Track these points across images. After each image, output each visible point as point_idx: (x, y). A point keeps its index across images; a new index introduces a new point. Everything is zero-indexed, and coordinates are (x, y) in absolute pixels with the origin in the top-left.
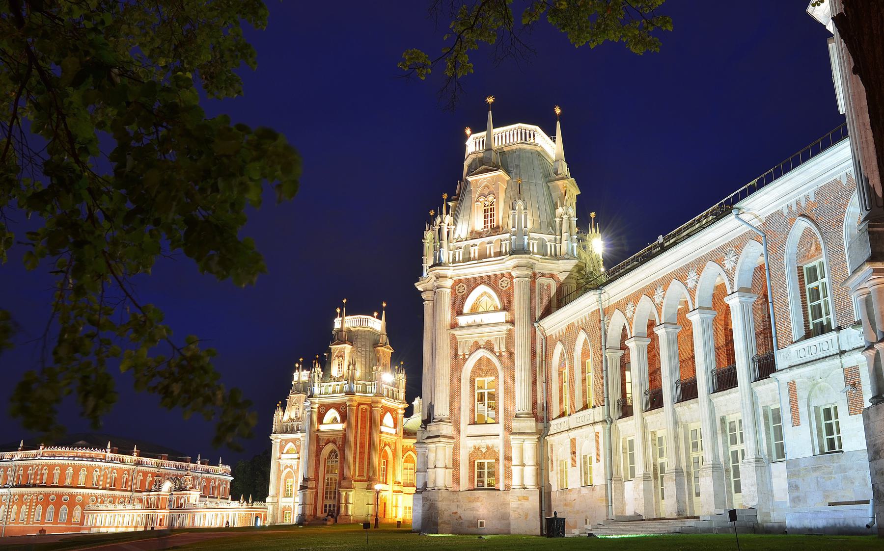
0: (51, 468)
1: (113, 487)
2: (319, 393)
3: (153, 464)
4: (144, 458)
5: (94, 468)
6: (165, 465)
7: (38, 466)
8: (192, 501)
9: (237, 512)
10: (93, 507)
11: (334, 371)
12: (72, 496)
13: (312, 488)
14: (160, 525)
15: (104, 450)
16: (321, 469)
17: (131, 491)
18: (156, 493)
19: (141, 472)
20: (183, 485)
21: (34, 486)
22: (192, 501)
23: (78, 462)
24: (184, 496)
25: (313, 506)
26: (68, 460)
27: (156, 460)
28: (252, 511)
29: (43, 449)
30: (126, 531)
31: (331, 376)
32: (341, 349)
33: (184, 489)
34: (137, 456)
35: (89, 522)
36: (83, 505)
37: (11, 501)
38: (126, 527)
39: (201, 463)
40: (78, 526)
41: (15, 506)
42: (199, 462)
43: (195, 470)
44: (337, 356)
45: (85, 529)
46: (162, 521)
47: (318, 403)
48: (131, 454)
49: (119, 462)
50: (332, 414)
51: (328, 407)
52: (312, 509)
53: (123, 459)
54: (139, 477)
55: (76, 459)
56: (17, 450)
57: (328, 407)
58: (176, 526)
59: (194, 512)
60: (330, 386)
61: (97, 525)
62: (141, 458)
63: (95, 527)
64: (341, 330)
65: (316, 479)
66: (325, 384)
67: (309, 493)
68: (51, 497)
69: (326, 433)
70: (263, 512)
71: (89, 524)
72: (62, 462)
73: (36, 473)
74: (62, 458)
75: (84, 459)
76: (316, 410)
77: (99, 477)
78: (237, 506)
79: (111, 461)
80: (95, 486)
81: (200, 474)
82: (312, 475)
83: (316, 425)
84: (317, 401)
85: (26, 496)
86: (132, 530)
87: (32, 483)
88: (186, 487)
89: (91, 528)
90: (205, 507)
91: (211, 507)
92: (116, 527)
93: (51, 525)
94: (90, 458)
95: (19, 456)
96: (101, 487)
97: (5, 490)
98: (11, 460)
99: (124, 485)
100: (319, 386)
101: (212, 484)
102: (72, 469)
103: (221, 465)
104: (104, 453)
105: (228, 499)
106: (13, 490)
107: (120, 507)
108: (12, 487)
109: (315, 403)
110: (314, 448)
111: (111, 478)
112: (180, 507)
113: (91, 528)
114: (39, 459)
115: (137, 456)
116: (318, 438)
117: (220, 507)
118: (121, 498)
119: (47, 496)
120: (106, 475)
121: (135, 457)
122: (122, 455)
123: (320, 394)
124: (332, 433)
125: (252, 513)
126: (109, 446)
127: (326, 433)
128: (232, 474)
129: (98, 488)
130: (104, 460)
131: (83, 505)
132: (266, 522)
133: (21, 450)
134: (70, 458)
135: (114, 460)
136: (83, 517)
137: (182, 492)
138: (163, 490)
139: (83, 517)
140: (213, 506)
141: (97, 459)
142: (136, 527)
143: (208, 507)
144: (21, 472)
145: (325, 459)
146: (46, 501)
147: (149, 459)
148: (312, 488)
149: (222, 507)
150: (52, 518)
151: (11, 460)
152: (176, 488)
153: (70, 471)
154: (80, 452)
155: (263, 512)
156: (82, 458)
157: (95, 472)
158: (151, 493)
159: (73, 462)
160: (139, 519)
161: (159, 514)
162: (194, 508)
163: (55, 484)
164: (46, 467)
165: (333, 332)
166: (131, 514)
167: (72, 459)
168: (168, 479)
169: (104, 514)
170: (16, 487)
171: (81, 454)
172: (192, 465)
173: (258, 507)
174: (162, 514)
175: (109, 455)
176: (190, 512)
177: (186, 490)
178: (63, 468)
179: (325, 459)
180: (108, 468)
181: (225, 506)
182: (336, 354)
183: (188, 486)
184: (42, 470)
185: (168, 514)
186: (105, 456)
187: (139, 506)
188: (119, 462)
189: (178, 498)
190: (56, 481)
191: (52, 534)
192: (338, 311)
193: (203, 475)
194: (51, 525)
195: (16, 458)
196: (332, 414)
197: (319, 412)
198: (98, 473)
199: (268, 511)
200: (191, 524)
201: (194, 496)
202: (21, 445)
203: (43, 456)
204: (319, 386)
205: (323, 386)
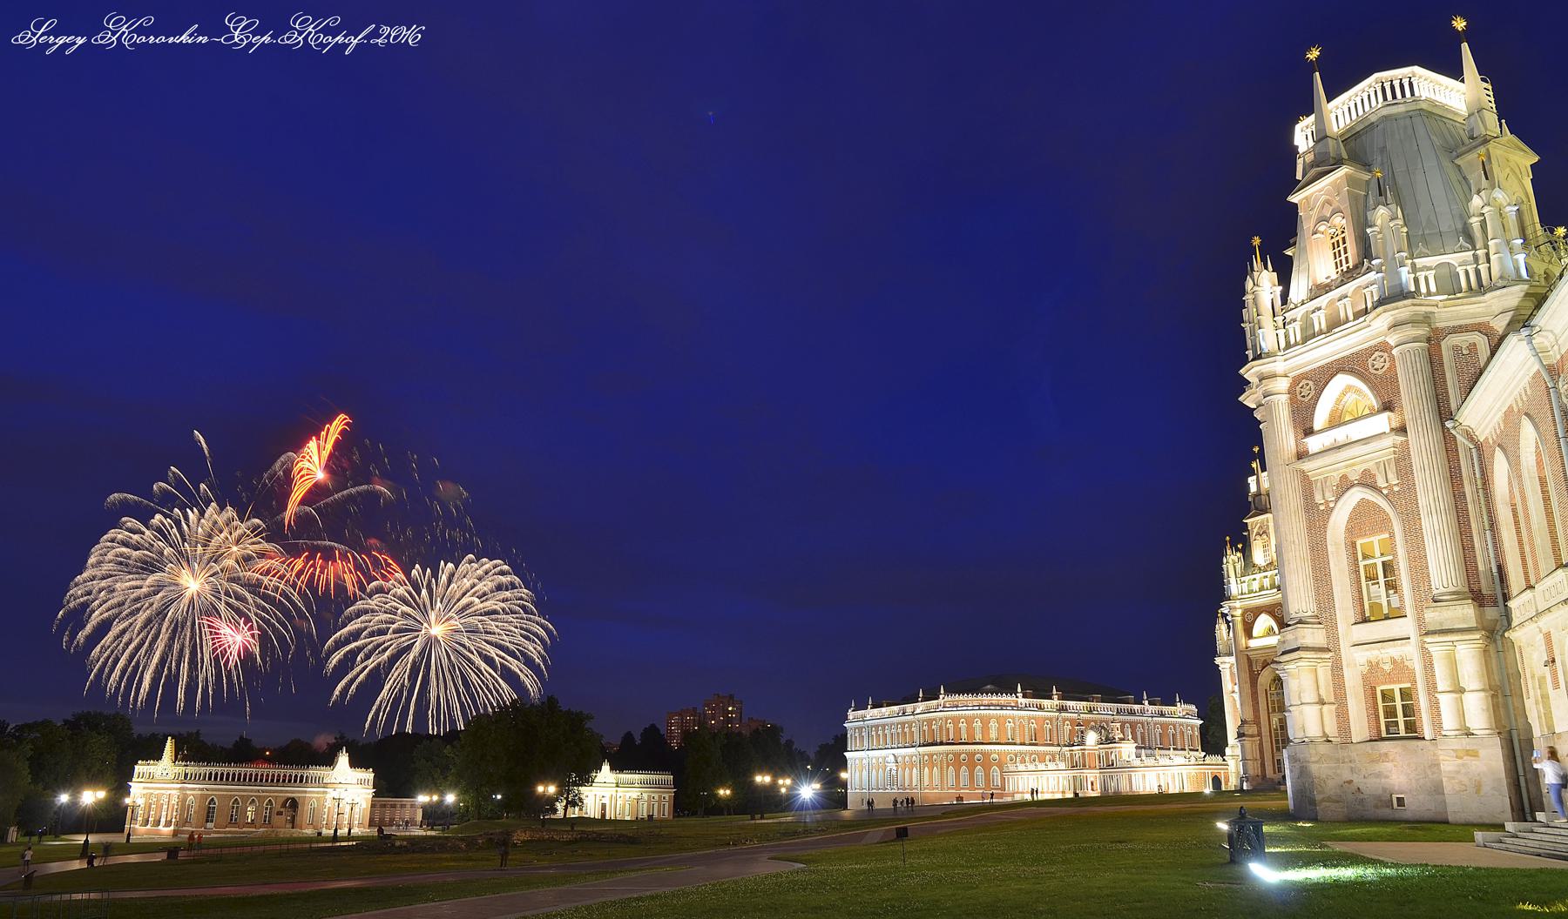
0: (956, 720)
2: (1240, 592)
5: (1005, 718)
7: (941, 719)
8: (1125, 757)
9: (1185, 771)
10: (1012, 768)
11: (1259, 557)
12: (986, 754)
13: (1252, 736)
14: (1093, 790)
17: (1059, 745)
18: (1079, 747)
19: (1067, 720)
20: (1110, 736)
21: (942, 744)
22: (1125, 757)
23: (985, 712)
25: (1259, 762)
27: (1085, 703)
28: (1205, 769)
31: (1254, 566)
32: (1262, 522)
33: (1112, 741)
34: (1058, 699)
35: (1010, 788)
36: (1000, 766)
38: (1053, 792)
39: (1150, 704)
41: (926, 768)
42: (1146, 702)
43: (1142, 712)
44: (1258, 534)
45: (1007, 795)
50: (1264, 622)
55: (982, 708)
56: (918, 702)
57: (1256, 612)
58: (1111, 791)
60: (1254, 579)
61: (1020, 790)
63: (1018, 793)
64: (1258, 494)
65: (1257, 721)
66: (1246, 579)
67: (1248, 742)
68: (963, 756)
69: (1260, 652)
70: (1221, 769)
71: (1011, 789)
72: (967, 712)
73: (941, 727)
74: (955, 709)
75: (991, 708)
76: (1239, 619)
77: (1013, 729)
78: (1184, 763)
79: (1026, 708)
81: (1150, 719)
82: (1249, 716)
83: (1243, 640)
84: (1238, 604)
86: (1059, 796)
88: (1114, 739)
90: (1142, 765)
91: (1149, 765)
92: (1053, 792)
95: (921, 709)
96: (1018, 742)
98: (913, 714)
100: (1239, 582)
101: (1171, 731)
103: (1179, 704)
104: (1015, 698)
105: (1197, 750)
106: (922, 750)
107: (1041, 766)
109: (1235, 608)
110: (1246, 676)
111: (1030, 729)
115: (1058, 699)
117: (1160, 764)
119: (957, 755)
120: (1022, 726)
121: (1056, 702)
122: (1039, 700)
123: (1242, 594)
124: (1267, 651)
126: (1019, 690)
127: (1260, 652)
128: (1199, 717)
129: (1015, 744)
130: (1016, 707)
131: (1000, 766)
132: (1230, 784)
134: (975, 708)
136: (1003, 779)
137: (1111, 745)
138: (1087, 743)
139: (1003, 779)
140: (1168, 762)
142: (1063, 792)
143: (1146, 765)
144: (926, 728)
146: (957, 761)
148: (1252, 736)
149: (1163, 764)
150: (967, 782)
153: (978, 725)
158: (1074, 748)
159: (979, 712)
160: (1066, 783)
161: (1088, 775)
162: (1129, 767)
165: (1250, 499)
167: (977, 708)
168: (1092, 728)
170: (924, 746)
172: (1136, 707)
173: (1214, 763)
174: (1092, 775)
175: (1022, 700)
176: (1125, 772)
178: (970, 721)
180: (1023, 718)
181: (1168, 762)
182: (1255, 531)
183: (1116, 737)
185: (1098, 775)
186: (1017, 702)
187: (1062, 766)
189: (1107, 753)
190: (964, 736)
191: (971, 802)
192: (1254, 465)
193: (1154, 719)
195: (918, 711)
196: (1264, 622)
197: (1244, 622)
200: (1141, 790)
201: (1127, 750)
202: (921, 695)
203: (944, 707)
204: (1239, 582)
205: (1244, 582)
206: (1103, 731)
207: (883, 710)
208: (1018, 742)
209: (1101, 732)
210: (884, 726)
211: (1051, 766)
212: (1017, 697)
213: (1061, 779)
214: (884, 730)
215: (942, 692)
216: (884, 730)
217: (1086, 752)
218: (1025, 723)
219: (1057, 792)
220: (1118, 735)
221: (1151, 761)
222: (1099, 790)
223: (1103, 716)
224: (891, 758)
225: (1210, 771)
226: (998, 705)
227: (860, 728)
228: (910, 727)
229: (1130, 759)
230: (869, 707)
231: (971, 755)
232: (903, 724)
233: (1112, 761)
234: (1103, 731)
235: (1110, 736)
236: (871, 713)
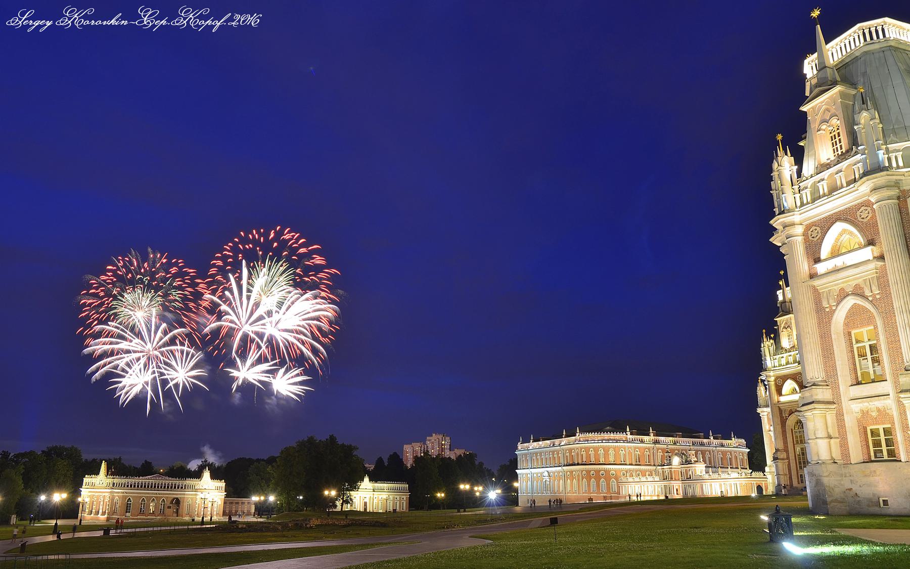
0: (587, 450)
1: (638, 463)
2: (773, 366)
3: (669, 441)
4: (660, 437)
5: (619, 448)
6: (680, 442)
7: (577, 449)
8: (698, 473)
9: (738, 482)
10: (624, 480)
11: (785, 342)
12: (607, 471)
14: (677, 494)
15: (624, 433)
16: (790, 439)
17: (654, 465)
18: (668, 467)
19: (660, 449)
20: (688, 459)
21: (578, 464)
24: (691, 468)
25: (788, 476)
26: (598, 443)
28: (752, 481)
29: (579, 436)
30: (652, 499)
31: (782, 348)
32: (787, 320)
33: (689, 462)
35: (624, 492)
36: (616, 479)
37: (565, 478)
40: (616, 495)
41: (569, 480)
42: (712, 438)
43: (709, 444)
44: (784, 328)
45: (622, 497)
46: (679, 491)
47: (774, 376)
48: (648, 435)
49: (639, 442)
50: (789, 385)
51: (784, 378)
52: (787, 479)
53: (642, 439)
54: (659, 453)
55: (604, 441)
56: (563, 438)
57: (784, 378)
58: (690, 494)
59: (701, 482)
60: (782, 357)
62: (658, 437)
64: (784, 302)
65: (786, 450)
66: (777, 357)
67: (780, 463)
69: (787, 404)
70: (763, 481)
71: (624, 493)
72: (594, 444)
73: (578, 454)
74: (586, 442)
75: (610, 441)
76: (773, 383)
77: (625, 455)
78: (737, 477)
79: (632, 441)
80: (623, 462)
81: (715, 448)
82: (781, 446)
83: (775, 397)
84: (772, 373)
85: (574, 472)
86: (655, 498)
87: (576, 463)
88: (691, 461)
89: (625, 496)
90: (710, 478)
91: (714, 478)
92: (650, 496)
93: (596, 495)
94: (614, 440)
95: (564, 442)
96: (628, 463)
97: (560, 468)
98: (559, 445)
99: (648, 461)
101: (729, 456)
102: (602, 450)
103: (733, 439)
104: (625, 435)
105: (746, 469)
107: (644, 479)
108: (564, 466)
109: (770, 376)
110: (778, 420)
111: (635, 455)
112: (689, 478)
113: (625, 496)
114: (577, 444)
116: (780, 410)
117: (722, 477)
118: (637, 471)
119: (588, 472)
120: (630, 453)
123: (774, 367)
124: (792, 404)
125: (753, 482)
126: (628, 430)
127: (787, 404)
128: (747, 447)
129: (626, 464)
130: (626, 441)
131: (616, 479)
132: (768, 490)
133: (565, 437)
134: (599, 442)
135: (635, 441)
141: (620, 440)
142: (658, 496)
143: (712, 478)
144: (568, 454)
145: (792, 429)
147: (664, 438)
150: (595, 489)
151: (559, 445)
152: (683, 462)
153: (601, 452)
154: (606, 436)
155: (763, 481)
156: (608, 440)
157: (621, 451)
158: (664, 467)
159: (602, 444)
161: (674, 485)
162: (700, 479)
163: (592, 463)
164: (583, 450)
165: (778, 305)
166: (653, 485)
167: (601, 441)
168: (676, 454)
169: (633, 485)
170: (567, 466)
171: (607, 438)
172: (705, 441)
175: (630, 437)
176: (698, 482)
177: (691, 464)
178: (596, 450)
179: (792, 429)
180: (631, 448)
181: (726, 476)
182: (782, 326)
183: (692, 460)
184: (581, 452)
185: (681, 485)
186: (627, 438)
187: (657, 479)
188: (639, 442)
189: (686, 471)
192: (781, 283)
193: (717, 448)
194: (596, 495)
195: (563, 444)
196: (789, 385)
197: (776, 385)
198: (623, 452)
199: (768, 480)
200: (710, 494)
201: (700, 468)
202: (564, 433)
206: (683, 456)
207: (540, 443)
208: (628, 463)
209: (682, 457)
210: (541, 453)
211: (650, 479)
212: (626, 434)
213: (656, 487)
214: (541, 455)
215: (578, 431)
216: (541, 455)
217: (673, 470)
218: (632, 451)
219: (654, 495)
220: (694, 459)
221: (716, 476)
222: (682, 495)
223: (683, 446)
224: (546, 474)
225: (755, 482)
226: (614, 440)
227: (525, 455)
228: (558, 454)
229: (702, 474)
230: (531, 441)
231: (598, 471)
232: (553, 452)
233: (690, 475)
234: (683, 456)
235: (688, 459)
236: (533, 445)
